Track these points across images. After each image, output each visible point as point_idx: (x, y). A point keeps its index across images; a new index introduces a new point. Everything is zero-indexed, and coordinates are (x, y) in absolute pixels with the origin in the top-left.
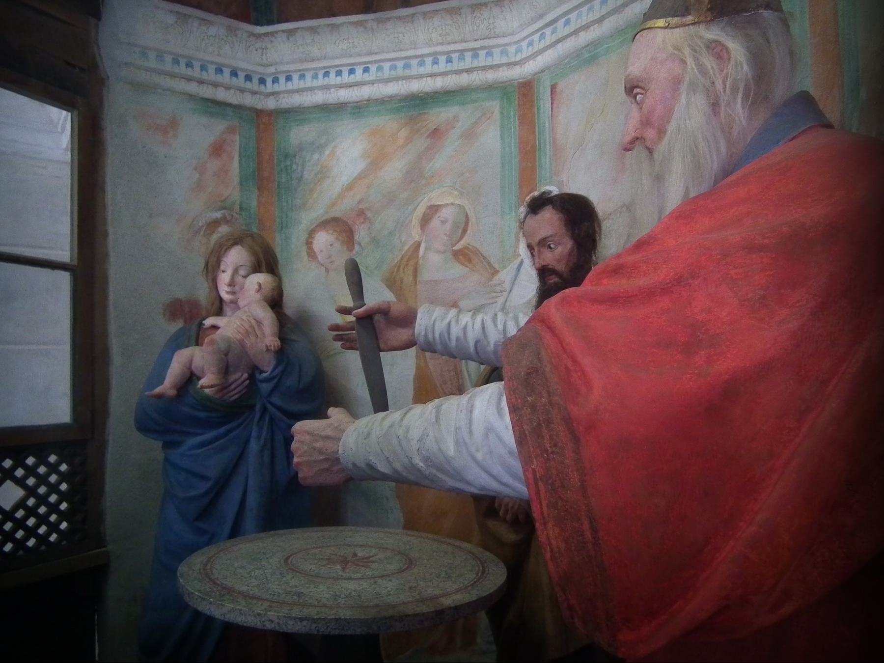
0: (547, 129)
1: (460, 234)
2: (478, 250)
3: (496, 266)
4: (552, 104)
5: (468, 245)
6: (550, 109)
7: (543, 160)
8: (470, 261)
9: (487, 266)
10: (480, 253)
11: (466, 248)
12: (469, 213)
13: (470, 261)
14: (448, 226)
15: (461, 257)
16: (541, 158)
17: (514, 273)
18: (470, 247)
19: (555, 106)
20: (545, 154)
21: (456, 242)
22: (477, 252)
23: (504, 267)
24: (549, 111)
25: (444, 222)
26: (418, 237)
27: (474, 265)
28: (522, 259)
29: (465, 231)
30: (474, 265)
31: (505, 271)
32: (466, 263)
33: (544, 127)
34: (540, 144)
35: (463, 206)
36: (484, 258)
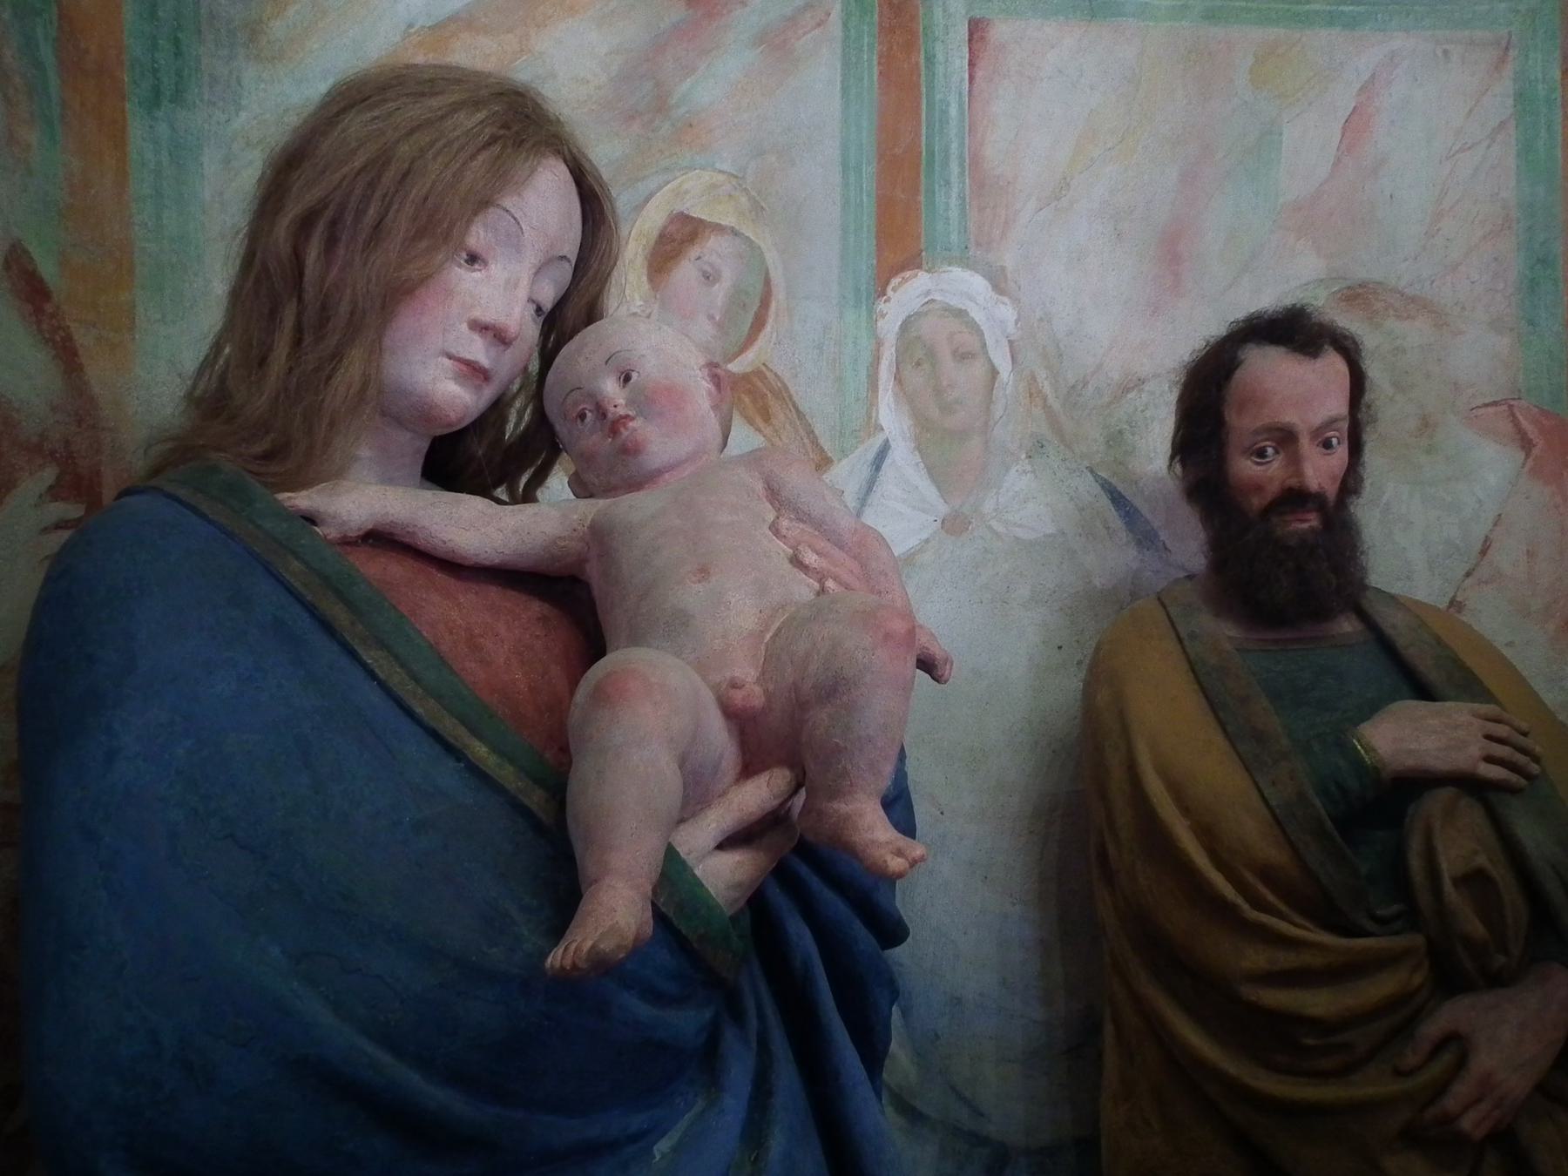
0: (953, 123)
1: (746, 328)
2: (786, 388)
3: (826, 444)
4: (972, 64)
5: (764, 368)
6: (967, 76)
7: (940, 199)
8: (767, 416)
9: (806, 441)
10: (790, 397)
11: (758, 373)
12: (772, 274)
13: (767, 416)
14: (720, 292)
15: (747, 400)
16: (934, 192)
17: (865, 472)
18: (768, 374)
19: (979, 74)
20: (948, 183)
21: (736, 349)
22: (783, 394)
23: (844, 453)
24: (962, 80)
25: (709, 278)
26: (639, 303)
27: (776, 431)
28: (887, 441)
29: (759, 324)
30: (776, 431)
31: (844, 462)
32: (759, 421)
33: (945, 112)
34: (931, 154)
35: (759, 248)
36: (800, 415)
